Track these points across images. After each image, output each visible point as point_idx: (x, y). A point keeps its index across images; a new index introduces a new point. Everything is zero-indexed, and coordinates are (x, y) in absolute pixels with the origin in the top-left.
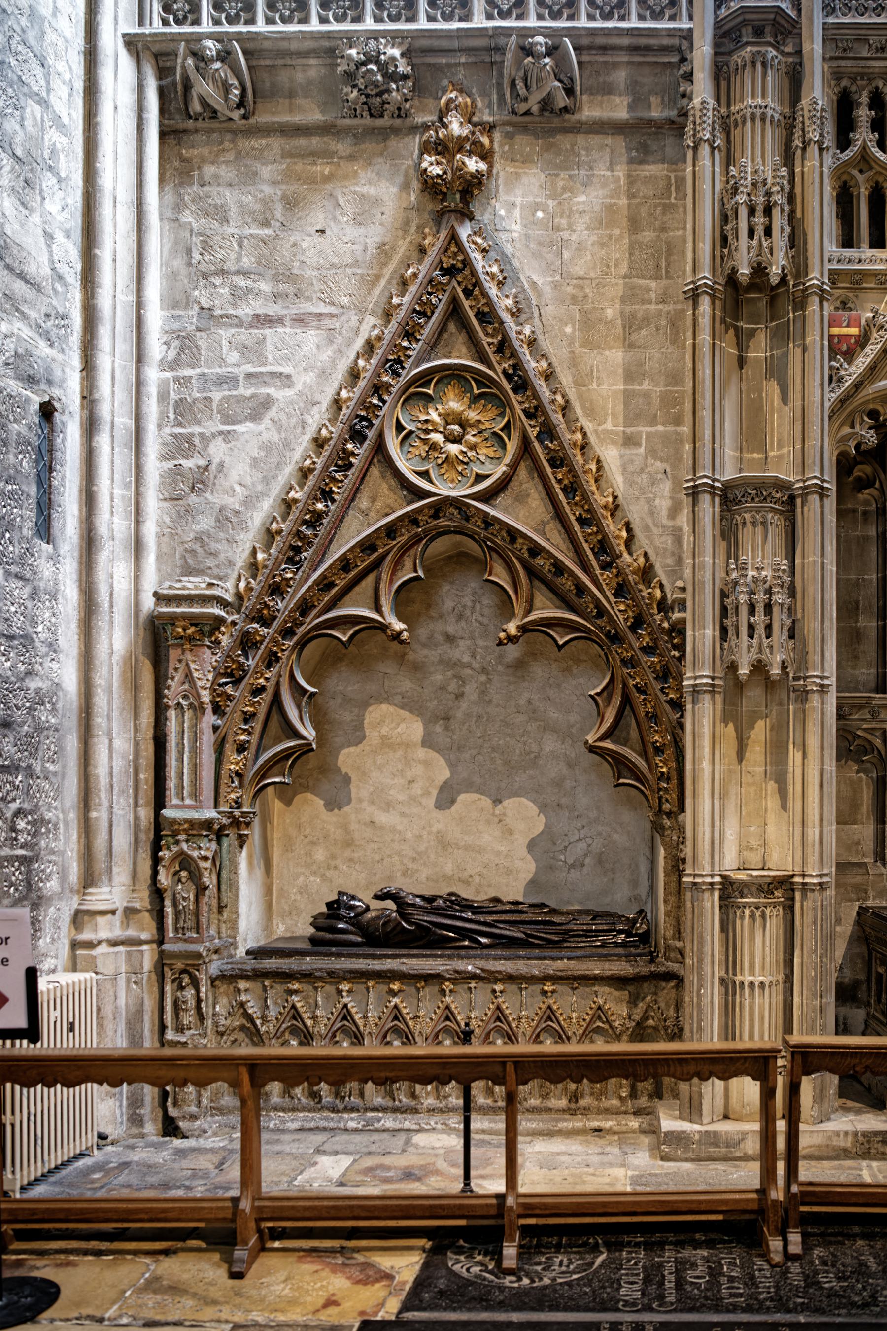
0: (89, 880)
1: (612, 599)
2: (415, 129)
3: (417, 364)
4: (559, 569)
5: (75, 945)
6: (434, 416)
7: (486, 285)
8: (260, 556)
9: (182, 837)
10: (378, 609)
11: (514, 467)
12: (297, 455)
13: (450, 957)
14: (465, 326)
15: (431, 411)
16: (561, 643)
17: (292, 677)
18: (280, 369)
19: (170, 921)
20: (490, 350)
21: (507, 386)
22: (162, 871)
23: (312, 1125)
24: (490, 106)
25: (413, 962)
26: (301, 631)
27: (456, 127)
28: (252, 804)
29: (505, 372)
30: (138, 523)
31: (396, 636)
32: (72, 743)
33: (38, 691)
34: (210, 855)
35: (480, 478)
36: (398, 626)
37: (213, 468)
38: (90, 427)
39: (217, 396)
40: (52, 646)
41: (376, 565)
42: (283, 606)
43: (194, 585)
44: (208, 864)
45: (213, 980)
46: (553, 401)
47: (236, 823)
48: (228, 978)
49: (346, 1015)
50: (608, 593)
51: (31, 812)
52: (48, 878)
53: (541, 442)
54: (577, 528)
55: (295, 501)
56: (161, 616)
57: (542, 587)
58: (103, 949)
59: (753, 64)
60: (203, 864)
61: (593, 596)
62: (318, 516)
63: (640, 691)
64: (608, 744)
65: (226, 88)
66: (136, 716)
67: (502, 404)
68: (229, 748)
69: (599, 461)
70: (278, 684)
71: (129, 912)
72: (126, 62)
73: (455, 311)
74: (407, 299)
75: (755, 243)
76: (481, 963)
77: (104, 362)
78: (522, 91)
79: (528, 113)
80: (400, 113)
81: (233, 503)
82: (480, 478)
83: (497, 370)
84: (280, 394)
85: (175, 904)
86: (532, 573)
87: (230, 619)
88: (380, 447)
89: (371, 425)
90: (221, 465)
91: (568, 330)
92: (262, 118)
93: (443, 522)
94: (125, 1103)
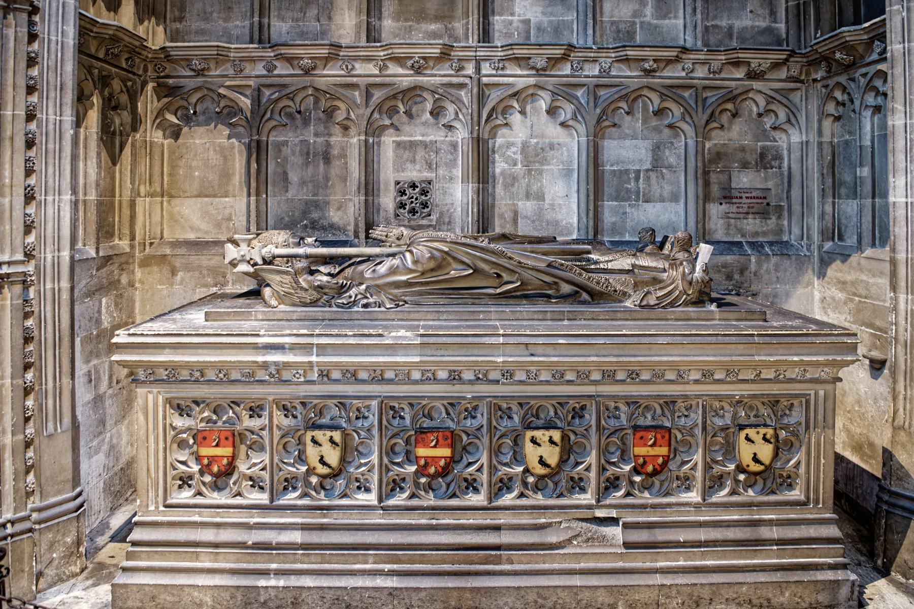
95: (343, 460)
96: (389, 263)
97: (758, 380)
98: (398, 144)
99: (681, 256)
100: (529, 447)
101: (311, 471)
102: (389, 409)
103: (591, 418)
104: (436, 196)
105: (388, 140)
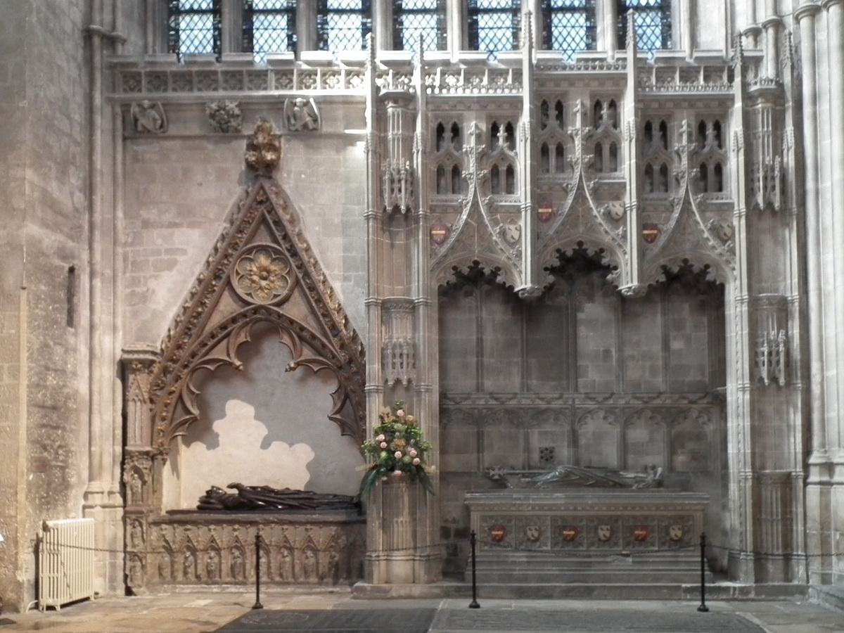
0: (91, 479)
1: (339, 350)
2: (243, 137)
3: (246, 244)
4: (314, 337)
8: (172, 333)
11: (292, 291)
12: (189, 286)
15: (253, 266)
16: (316, 370)
17: (188, 387)
18: (180, 247)
20: (280, 238)
23: (196, 590)
24: (279, 127)
25: (241, 515)
27: (261, 139)
28: (169, 445)
29: (286, 248)
30: (114, 317)
31: (237, 368)
32: (84, 417)
33: (68, 393)
34: (148, 467)
36: (238, 363)
37: (150, 291)
38: (92, 275)
40: (75, 374)
41: (227, 335)
42: (183, 354)
43: (140, 346)
46: (309, 262)
48: (156, 523)
49: (213, 540)
50: (337, 348)
52: (72, 476)
53: (304, 280)
54: (321, 318)
55: (188, 307)
56: (126, 360)
57: (307, 346)
60: (144, 471)
61: (330, 350)
62: (199, 314)
63: (354, 392)
67: (286, 262)
68: (157, 420)
69: (331, 288)
70: (181, 390)
71: (111, 493)
74: (240, 215)
76: (276, 515)
79: (297, 130)
80: (237, 130)
81: (160, 307)
82: (276, 296)
83: (284, 247)
84: (180, 258)
85: (132, 490)
86: (301, 338)
87: (158, 360)
88: (229, 283)
89: (224, 272)
90: (153, 291)
91: (317, 228)
92: (172, 130)
93: (258, 316)
94: (107, 580)
97: (675, 510)
102: (554, 519)
103: (620, 523)
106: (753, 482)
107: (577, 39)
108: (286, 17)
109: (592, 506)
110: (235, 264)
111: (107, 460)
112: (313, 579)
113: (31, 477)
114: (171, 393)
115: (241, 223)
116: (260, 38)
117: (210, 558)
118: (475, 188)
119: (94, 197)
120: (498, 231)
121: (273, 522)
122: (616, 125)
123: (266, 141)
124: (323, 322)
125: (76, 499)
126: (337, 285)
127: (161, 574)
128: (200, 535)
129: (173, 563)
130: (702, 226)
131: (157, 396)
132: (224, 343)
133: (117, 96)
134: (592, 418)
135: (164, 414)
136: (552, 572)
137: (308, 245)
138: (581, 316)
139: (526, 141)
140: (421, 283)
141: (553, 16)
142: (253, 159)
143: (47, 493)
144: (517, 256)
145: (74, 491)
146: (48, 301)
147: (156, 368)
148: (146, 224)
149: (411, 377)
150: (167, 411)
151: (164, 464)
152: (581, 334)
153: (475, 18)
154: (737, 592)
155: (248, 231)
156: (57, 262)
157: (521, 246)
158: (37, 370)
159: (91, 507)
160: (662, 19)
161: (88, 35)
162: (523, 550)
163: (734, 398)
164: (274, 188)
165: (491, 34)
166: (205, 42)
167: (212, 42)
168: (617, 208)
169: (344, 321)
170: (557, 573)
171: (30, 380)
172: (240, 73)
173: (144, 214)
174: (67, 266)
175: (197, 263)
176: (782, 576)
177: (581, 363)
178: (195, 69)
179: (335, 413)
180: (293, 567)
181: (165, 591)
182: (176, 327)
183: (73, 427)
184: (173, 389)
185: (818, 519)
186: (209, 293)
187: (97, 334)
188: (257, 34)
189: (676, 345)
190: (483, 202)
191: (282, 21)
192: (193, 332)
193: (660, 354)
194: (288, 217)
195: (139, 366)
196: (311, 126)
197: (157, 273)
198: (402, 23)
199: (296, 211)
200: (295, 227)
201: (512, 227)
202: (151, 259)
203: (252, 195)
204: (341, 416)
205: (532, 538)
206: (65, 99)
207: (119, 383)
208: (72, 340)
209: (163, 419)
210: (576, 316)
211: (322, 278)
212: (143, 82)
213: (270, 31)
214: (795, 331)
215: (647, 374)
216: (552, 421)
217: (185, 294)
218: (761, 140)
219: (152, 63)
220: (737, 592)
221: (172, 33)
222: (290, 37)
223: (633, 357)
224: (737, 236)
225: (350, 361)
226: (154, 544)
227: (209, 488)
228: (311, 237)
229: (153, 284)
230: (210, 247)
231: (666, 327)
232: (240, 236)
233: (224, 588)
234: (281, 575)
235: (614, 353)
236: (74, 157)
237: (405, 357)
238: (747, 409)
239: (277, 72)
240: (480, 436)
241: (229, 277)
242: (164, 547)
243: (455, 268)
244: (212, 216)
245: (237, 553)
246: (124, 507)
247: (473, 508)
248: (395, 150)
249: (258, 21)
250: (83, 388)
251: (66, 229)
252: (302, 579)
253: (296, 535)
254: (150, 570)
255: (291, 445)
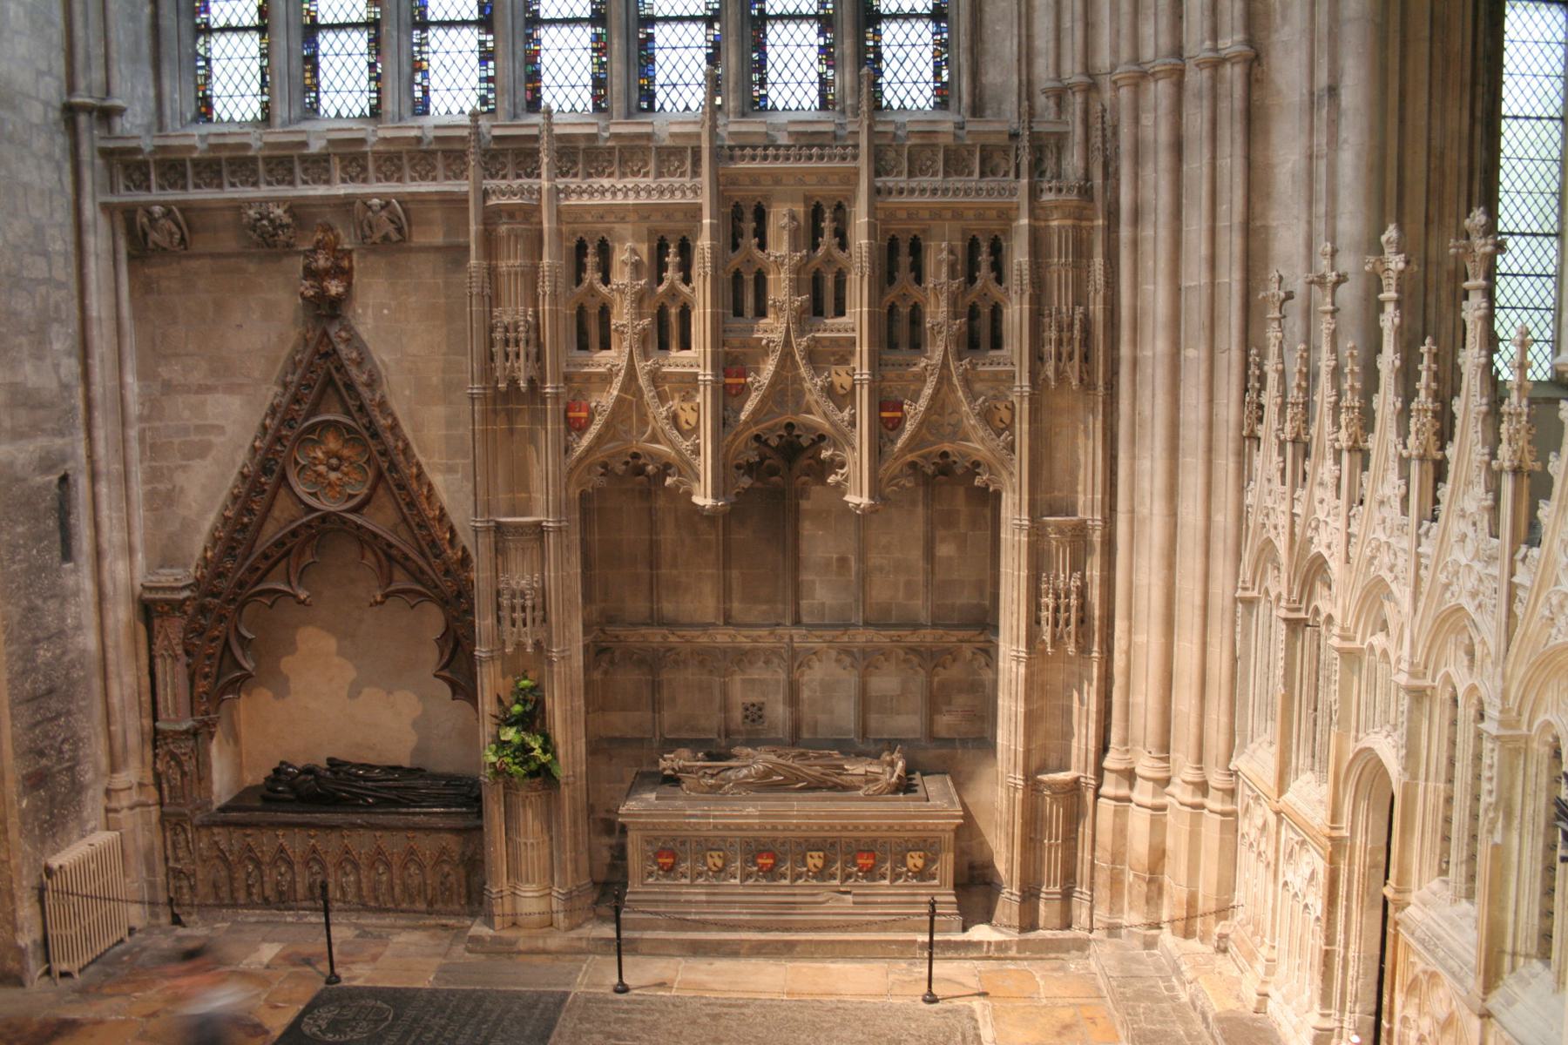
0: (114, 768)
2: (299, 253)
3: (306, 419)
4: (407, 557)
5: (108, 810)
6: (320, 455)
7: (349, 368)
9: (170, 740)
10: (289, 583)
11: (373, 489)
12: (230, 483)
13: (347, 813)
14: (337, 390)
17: (236, 629)
18: (217, 422)
19: (166, 793)
20: (353, 409)
21: (366, 434)
22: (159, 763)
23: (264, 919)
24: (349, 236)
26: (240, 598)
27: (322, 262)
29: (364, 426)
30: (129, 534)
32: (96, 683)
35: (351, 497)
37: (177, 489)
38: (94, 477)
39: (176, 441)
41: (288, 553)
44: (187, 758)
45: (197, 827)
46: (396, 447)
47: (206, 724)
49: (282, 850)
51: (72, 737)
58: (125, 812)
59: (509, 236)
60: (183, 758)
62: (245, 526)
64: (442, 673)
65: (171, 234)
66: (137, 659)
67: (365, 446)
71: (141, 785)
72: (103, 223)
73: (329, 381)
74: (296, 378)
75: (508, 364)
77: (100, 434)
78: (368, 232)
82: (351, 497)
84: (216, 439)
85: (168, 781)
86: (390, 558)
88: (283, 477)
89: (277, 463)
90: (182, 490)
91: (407, 393)
92: (198, 246)
93: (328, 526)
95: (724, 865)
96: (745, 771)
98: (744, 681)
99: (888, 769)
100: (809, 860)
101: (710, 869)
104: (767, 712)
105: (738, 678)
106: (1024, 793)
107: (805, 65)
108: (366, 35)
109: (798, 826)
110: (292, 449)
111: (133, 739)
112: (423, 906)
113: (24, 804)
114: (213, 639)
115: (298, 388)
116: (328, 68)
117: (281, 875)
118: (631, 347)
119: (90, 361)
120: (664, 414)
121: (361, 826)
122: (843, 245)
123: (329, 264)
124: (419, 536)
125: (93, 804)
126: (438, 480)
127: (217, 895)
128: (265, 843)
129: (231, 879)
130: (965, 408)
131: (195, 645)
132: (282, 565)
133: (115, 199)
134: (820, 661)
135: (207, 670)
136: (742, 917)
137: (395, 419)
138: (805, 505)
139: (705, 277)
140: (550, 498)
141: (769, 28)
142: (312, 293)
143: (52, 815)
144: (693, 452)
145: (90, 792)
146: (30, 543)
147: (190, 610)
148: (168, 387)
149: (540, 637)
150: (210, 666)
151: (212, 738)
152: (806, 533)
153: (650, 31)
154: (992, 948)
155: (310, 397)
156: (39, 480)
157: (698, 438)
158: (21, 652)
159: (116, 811)
160: (934, 34)
161: (70, 112)
162: (702, 886)
163: (1007, 666)
164: (343, 334)
165: (674, 57)
166: (248, 78)
167: (259, 77)
168: (841, 379)
169: (448, 536)
170: (748, 917)
171: (10, 672)
172: (290, 159)
173: (164, 372)
174: (54, 478)
175: (241, 446)
176: (1057, 921)
177: (806, 576)
178: (225, 154)
179: (442, 669)
180: (393, 889)
181: (224, 920)
182: (214, 546)
183: (82, 703)
184: (216, 633)
185: (1109, 849)
186: (258, 494)
187: (106, 564)
188: (323, 63)
189: (945, 550)
190: (643, 367)
191: (360, 40)
192: (238, 551)
193: (921, 563)
194: (365, 377)
195: (166, 608)
196: (395, 236)
197: (184, 463)
198: (538, 41)
199: (375, 366)
200: (373, 391)
201: (686, 406)
202: (176, 441)
203: (313, 344)
204: (451, 672)
205: (714, 869)
206: (39, 230)
207: (142, 629)
208: (70, 581)
209: (206, 676)
210: (798, 505)
211: (414, 470)
212: (153, 177)
213: (344, 58)
214: (1094, 571)
215: (901, 595)
216: (760, 664)
217: (223, 496)
218: (1056, 276)
219: (164, 148)
220: (992, 948)
221: (201, 63)
222: (372, 66)
223: (881, 569)
224: (1017, 426)
225: (459, 595)
226: (205, 853)
227: (276, 765)
228: (398, 407)
229: (180, 478)
230: (257, 421)
231: (931, 524)
232: (297, 407)
233: (300, 917)
234: (377, 899)
235: (853, 563)
236: (57, 308)
237: (528, 610)
238: (1021, 688)
239: (342, 157)
240: (656, 686)
241: (284, 469)
242: (218, 857)
243: (605, 465)
244: (257, 374)
245: (316, 868)
246: (162, 804)
247: (631, 827)
248: (513, 290)
249: (326, 41)
250: (90, 641)
251: (48, 426)
252: (404, 906)
253: (394, 844)
254: (203, 889)
255: (390, 693)
